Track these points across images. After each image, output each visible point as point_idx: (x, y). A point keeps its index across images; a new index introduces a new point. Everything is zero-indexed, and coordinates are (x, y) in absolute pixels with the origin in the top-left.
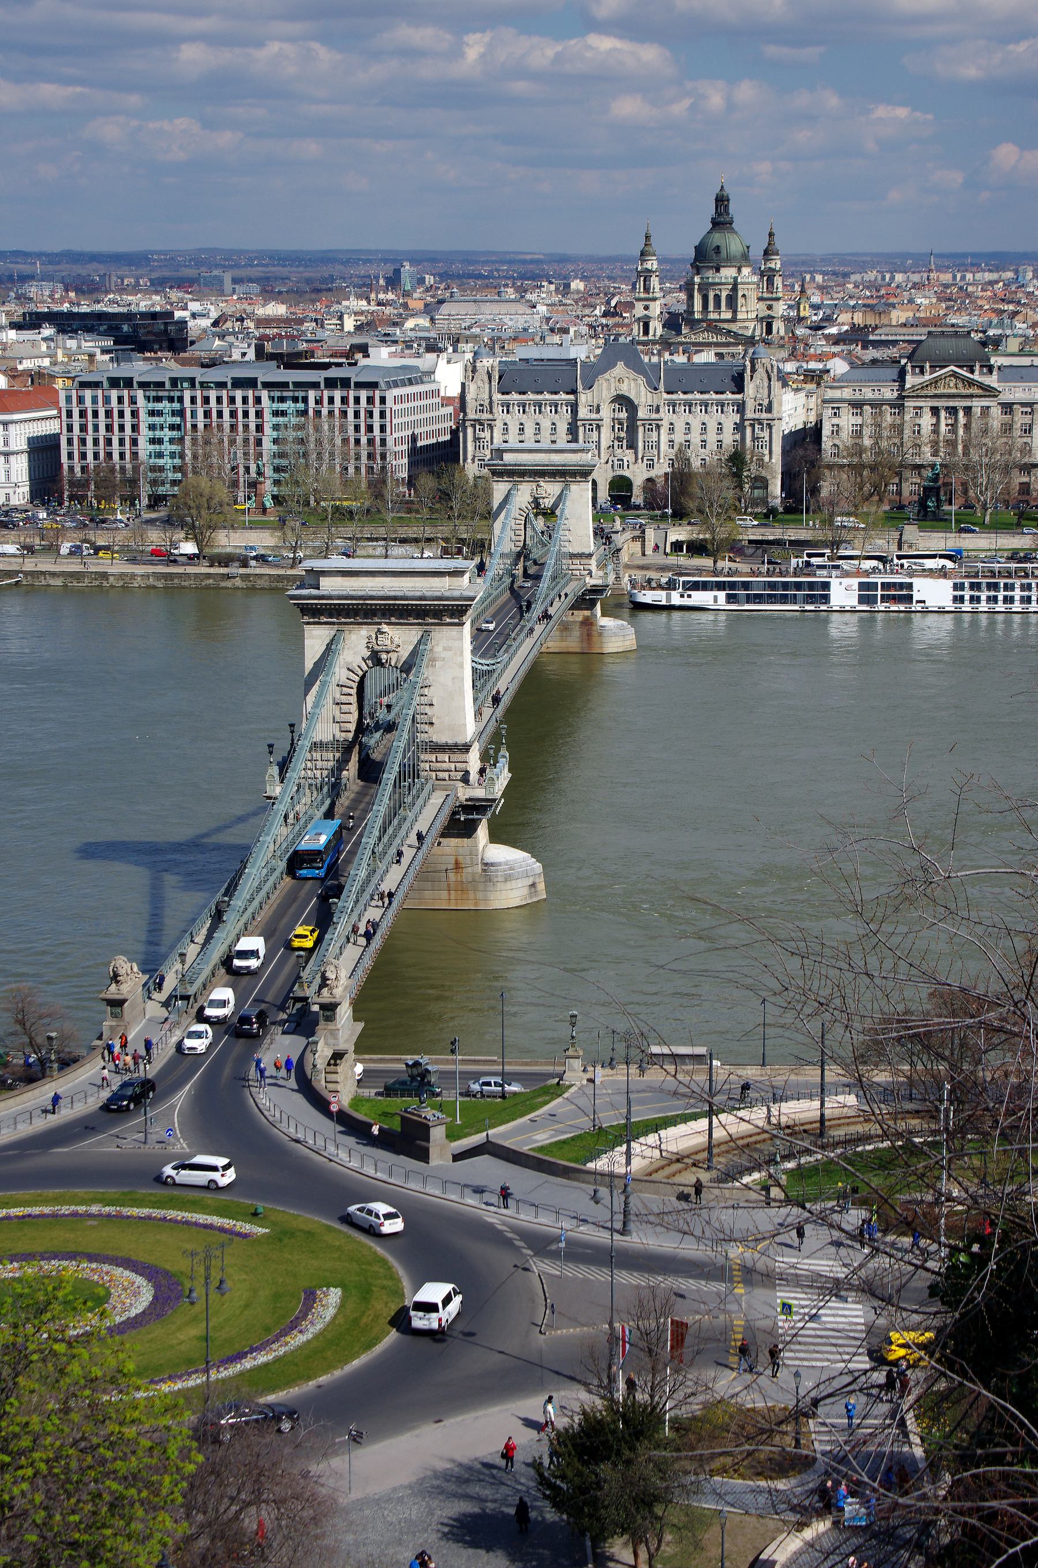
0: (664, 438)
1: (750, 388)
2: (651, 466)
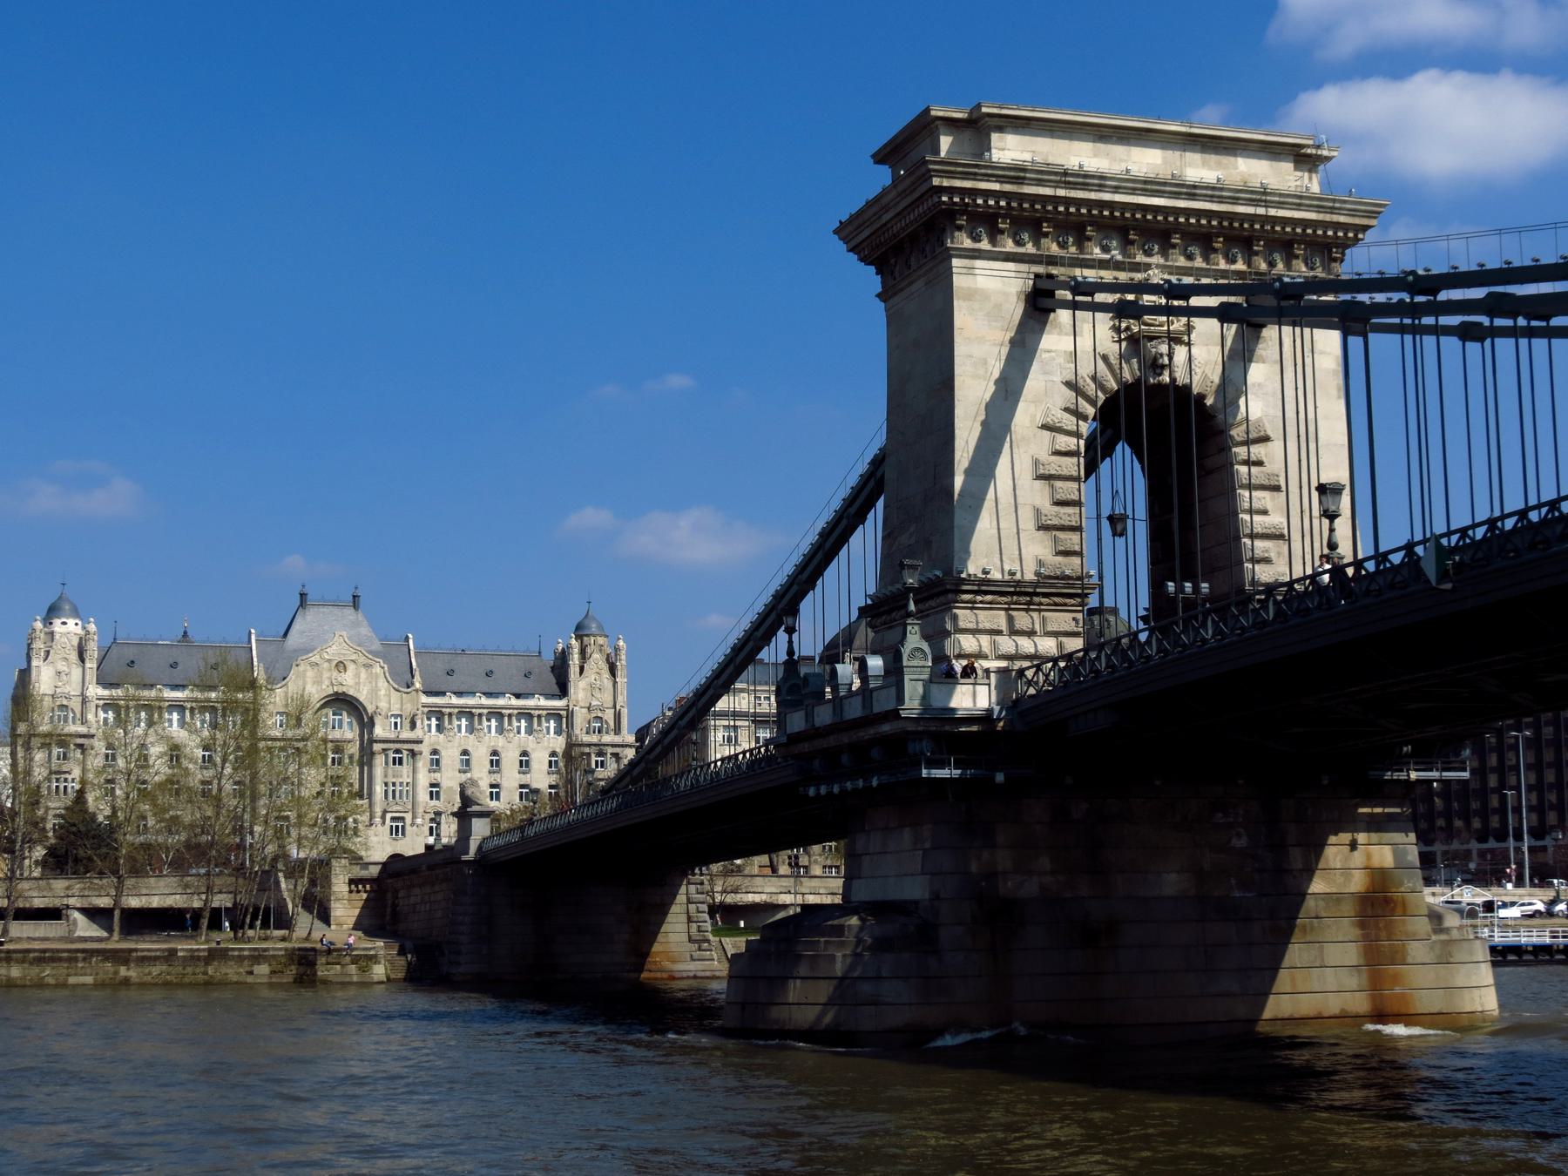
0: (424, 779)
1: (579, 689)
2: (398, 831)
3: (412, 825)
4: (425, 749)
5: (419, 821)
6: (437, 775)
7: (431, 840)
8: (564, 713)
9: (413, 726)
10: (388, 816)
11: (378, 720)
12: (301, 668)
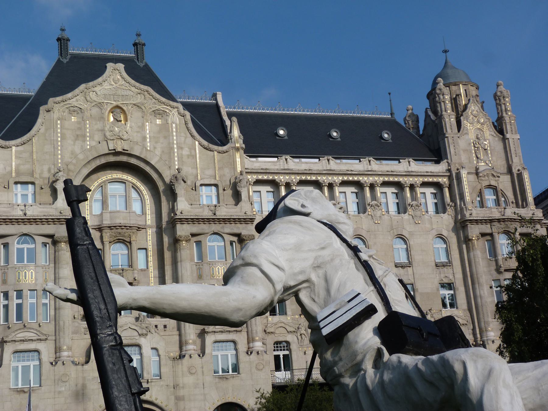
3: (249, 352)
5: (258, 345)
7: (282, 376)
8: (444, 181)
9: (237, 196)
11: (180, 189)
12: (55, 114)
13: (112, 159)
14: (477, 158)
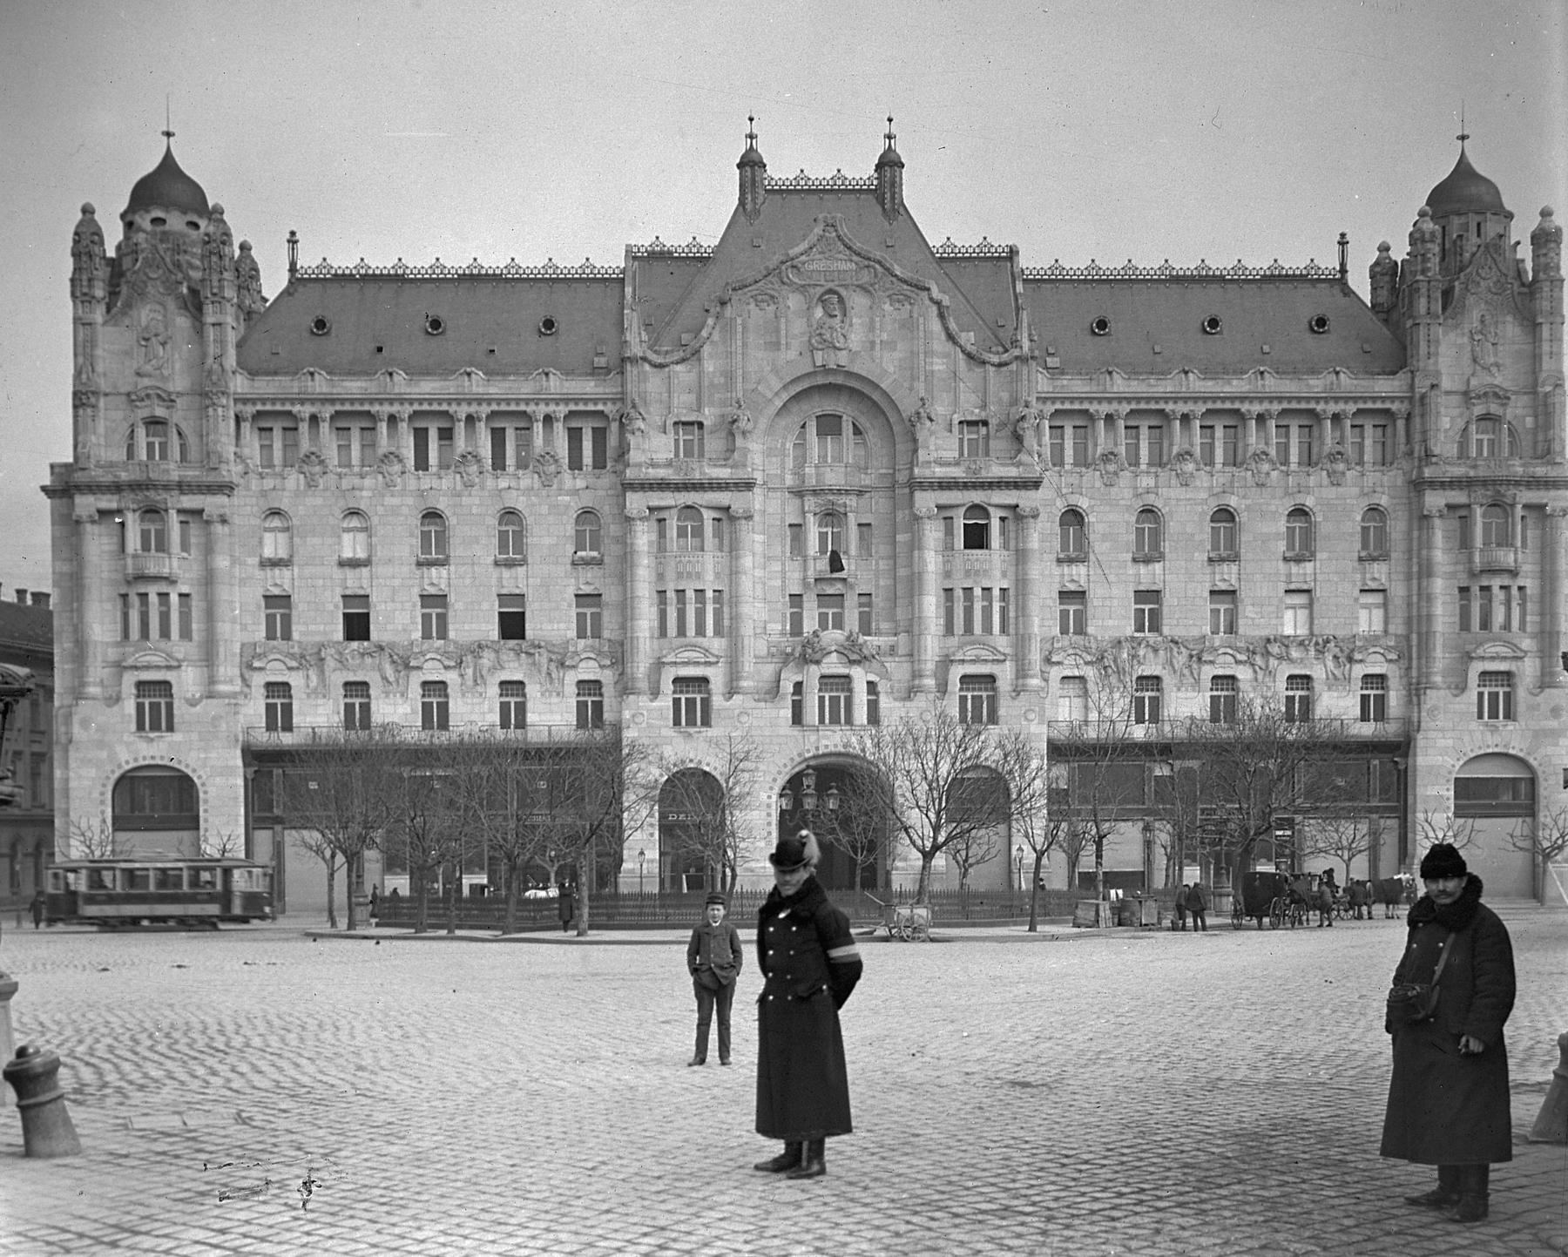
0: (1046, 578)
4: (1046, 503)
6: (1079, 571)
10: (957, 672)
13: (820, 380)
14: (1475, 360)
